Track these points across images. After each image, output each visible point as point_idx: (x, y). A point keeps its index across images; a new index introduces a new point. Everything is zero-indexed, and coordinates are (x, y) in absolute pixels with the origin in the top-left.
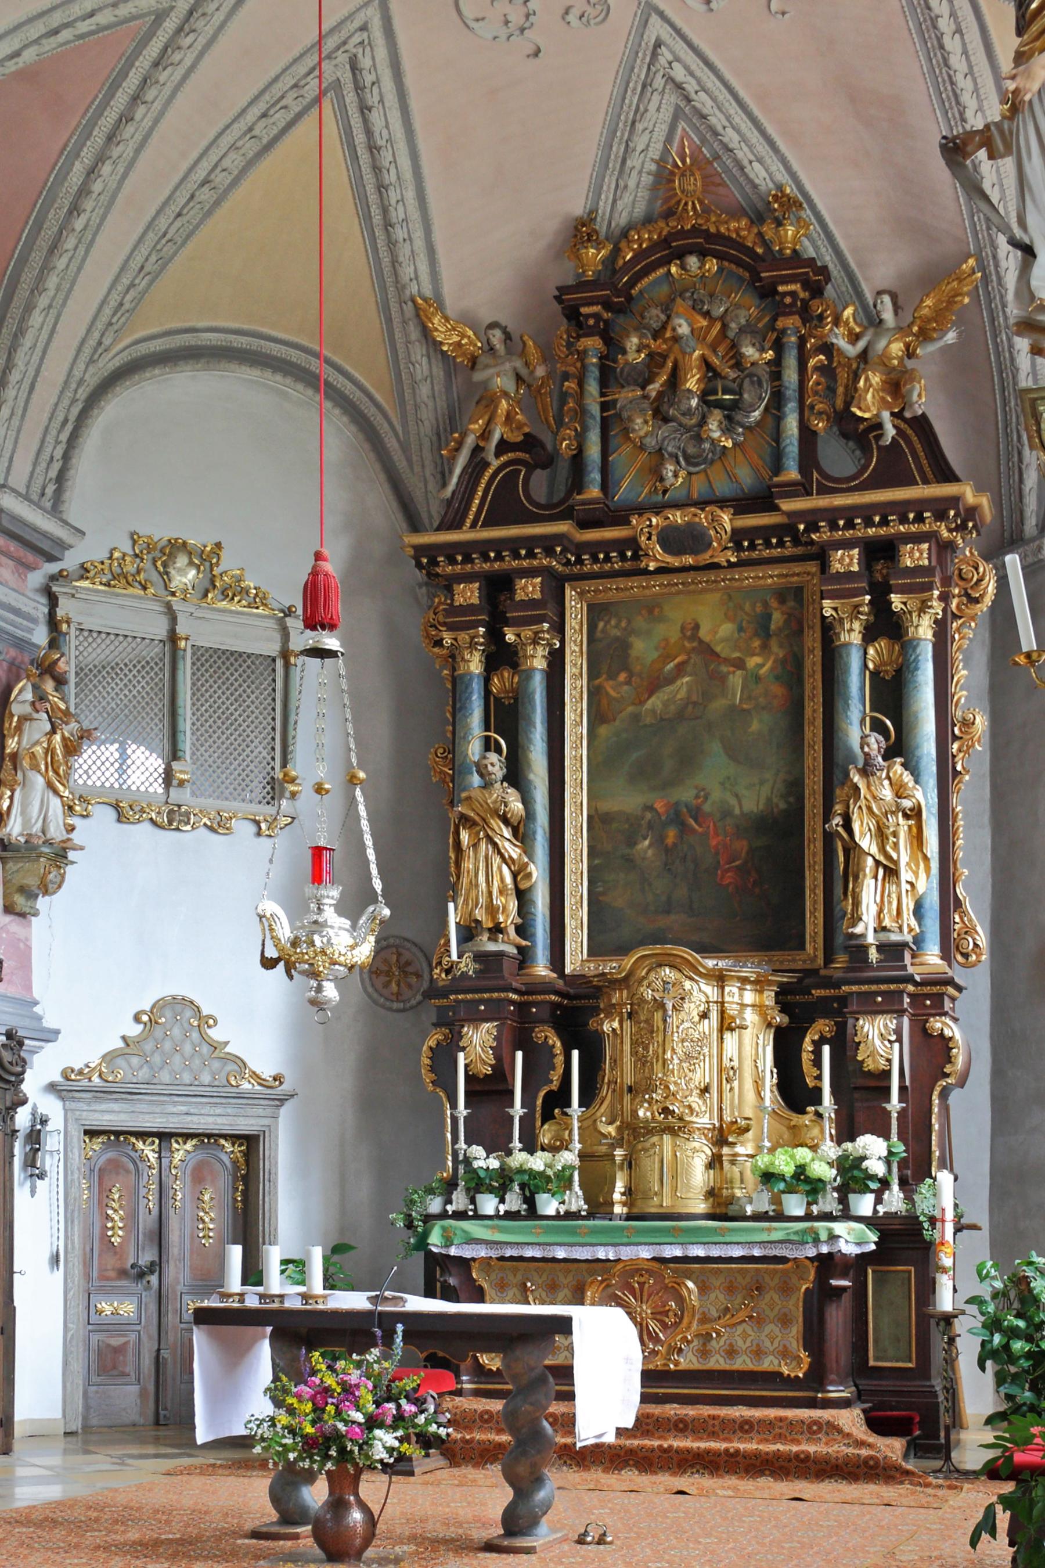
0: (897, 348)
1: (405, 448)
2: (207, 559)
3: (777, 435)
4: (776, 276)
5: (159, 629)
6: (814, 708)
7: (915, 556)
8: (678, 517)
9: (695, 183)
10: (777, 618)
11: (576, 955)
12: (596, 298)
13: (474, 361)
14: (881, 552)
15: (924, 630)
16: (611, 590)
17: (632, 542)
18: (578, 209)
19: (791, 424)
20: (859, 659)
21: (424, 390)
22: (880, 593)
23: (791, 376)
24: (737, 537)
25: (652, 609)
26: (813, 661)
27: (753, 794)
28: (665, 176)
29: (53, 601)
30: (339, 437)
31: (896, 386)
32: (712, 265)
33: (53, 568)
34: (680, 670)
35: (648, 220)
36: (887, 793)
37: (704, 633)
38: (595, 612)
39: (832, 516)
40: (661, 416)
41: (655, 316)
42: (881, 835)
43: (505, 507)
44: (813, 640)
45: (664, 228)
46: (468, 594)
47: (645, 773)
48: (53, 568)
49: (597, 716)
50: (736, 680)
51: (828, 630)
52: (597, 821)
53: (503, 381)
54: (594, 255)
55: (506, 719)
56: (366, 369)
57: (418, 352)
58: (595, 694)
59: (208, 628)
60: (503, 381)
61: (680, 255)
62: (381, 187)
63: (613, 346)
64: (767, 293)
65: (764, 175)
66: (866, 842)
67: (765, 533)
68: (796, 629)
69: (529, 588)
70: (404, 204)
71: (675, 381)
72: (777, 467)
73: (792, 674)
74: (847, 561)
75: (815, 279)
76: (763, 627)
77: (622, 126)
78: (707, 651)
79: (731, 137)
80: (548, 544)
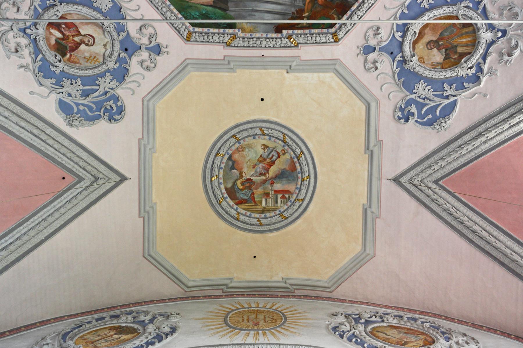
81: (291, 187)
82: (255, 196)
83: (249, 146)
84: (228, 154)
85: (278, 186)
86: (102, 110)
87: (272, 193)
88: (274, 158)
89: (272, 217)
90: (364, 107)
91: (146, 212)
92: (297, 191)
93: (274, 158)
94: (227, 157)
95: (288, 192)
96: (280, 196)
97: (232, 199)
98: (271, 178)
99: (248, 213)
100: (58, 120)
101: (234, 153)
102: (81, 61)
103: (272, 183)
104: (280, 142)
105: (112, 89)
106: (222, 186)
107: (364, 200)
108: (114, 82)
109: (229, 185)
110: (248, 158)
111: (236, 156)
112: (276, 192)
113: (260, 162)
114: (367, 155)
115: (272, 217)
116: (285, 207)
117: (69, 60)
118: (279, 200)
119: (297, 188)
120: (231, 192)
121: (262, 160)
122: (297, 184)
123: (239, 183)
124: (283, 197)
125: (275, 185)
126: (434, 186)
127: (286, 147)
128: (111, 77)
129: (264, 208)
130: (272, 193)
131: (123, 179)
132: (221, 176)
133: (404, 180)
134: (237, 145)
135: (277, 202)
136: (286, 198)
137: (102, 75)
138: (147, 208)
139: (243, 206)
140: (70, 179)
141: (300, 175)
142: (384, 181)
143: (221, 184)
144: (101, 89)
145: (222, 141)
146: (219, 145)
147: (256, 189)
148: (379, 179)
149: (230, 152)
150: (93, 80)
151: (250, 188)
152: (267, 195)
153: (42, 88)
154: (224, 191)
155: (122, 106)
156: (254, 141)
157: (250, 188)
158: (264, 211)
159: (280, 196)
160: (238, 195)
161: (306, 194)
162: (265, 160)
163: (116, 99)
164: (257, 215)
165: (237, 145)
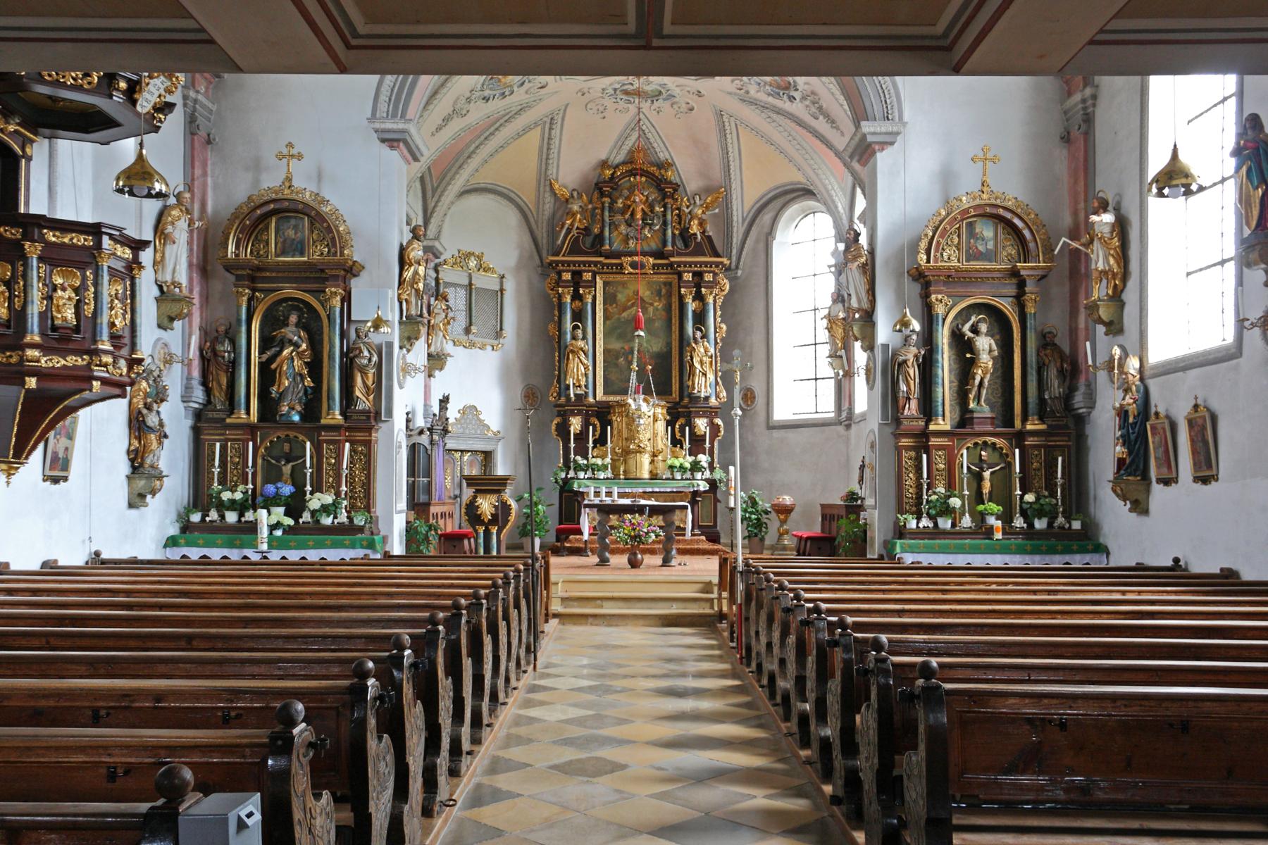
0: (700, 212)
1: (536, 222)
2: (479, 258)
3: (665, 234)
4: (665, 188)
5: (466, 282)
6: (675, 321)
7: (708, 277)
8: (636, 258)
9: (641, 155)
10: (664, 291)
12: (605, 186)
13: (567, 200)
14: (698, 275)
15: (710, 300)
16: (611, 278)
17: (621, 265)
18: (604, 157)
19: (669, 232)
20: (691, 306)
21: (547, 206)
22: (698, 286)
23: (669, 217)
24: (654, 265)
25: (624, 284)
26: (675, 306)
27: (657, 346)
28: (631, 152)
29: (437, 272)
31: (701, 223)
32: (644, 179)
33: (437, 261)
34: (633, 305)
35: (624, 163)
36: (702, 350)
37: (641, 293)
38: (606, 284)
39: (685, 264)
41: (626, 193)
42: (701, 363)
43: (575, 249)
44: (675, 300)
45: (629, 167)
46: (567, 276)
47: (621, 337)
48: (437, 261)
49: (606, 318)
50: (651, 309)
51: (681, 298)
52: (606, 351)
53: (576, 208)
54: (608, 173)
55: (578, 316)
56: (528, 197)
57: (548, 195)
58: (605, 310)
60: (576, 208)
61: (635, 175)
62: (548, 149)
63: (613, 202)
64: (660, 189)
65: (663, 156)
66: (697, 365)
67: (662, 265)
68: (669, 295)
70: (554, 155)
71: (633, 214)
72: (665, 244)
73: (668, 308)
74: (688, 277)
75: (676, 187)
76: (659, 293)
77: (623, 137)
78: (642, 299)
79: (655, 145)
80: (596, 263)
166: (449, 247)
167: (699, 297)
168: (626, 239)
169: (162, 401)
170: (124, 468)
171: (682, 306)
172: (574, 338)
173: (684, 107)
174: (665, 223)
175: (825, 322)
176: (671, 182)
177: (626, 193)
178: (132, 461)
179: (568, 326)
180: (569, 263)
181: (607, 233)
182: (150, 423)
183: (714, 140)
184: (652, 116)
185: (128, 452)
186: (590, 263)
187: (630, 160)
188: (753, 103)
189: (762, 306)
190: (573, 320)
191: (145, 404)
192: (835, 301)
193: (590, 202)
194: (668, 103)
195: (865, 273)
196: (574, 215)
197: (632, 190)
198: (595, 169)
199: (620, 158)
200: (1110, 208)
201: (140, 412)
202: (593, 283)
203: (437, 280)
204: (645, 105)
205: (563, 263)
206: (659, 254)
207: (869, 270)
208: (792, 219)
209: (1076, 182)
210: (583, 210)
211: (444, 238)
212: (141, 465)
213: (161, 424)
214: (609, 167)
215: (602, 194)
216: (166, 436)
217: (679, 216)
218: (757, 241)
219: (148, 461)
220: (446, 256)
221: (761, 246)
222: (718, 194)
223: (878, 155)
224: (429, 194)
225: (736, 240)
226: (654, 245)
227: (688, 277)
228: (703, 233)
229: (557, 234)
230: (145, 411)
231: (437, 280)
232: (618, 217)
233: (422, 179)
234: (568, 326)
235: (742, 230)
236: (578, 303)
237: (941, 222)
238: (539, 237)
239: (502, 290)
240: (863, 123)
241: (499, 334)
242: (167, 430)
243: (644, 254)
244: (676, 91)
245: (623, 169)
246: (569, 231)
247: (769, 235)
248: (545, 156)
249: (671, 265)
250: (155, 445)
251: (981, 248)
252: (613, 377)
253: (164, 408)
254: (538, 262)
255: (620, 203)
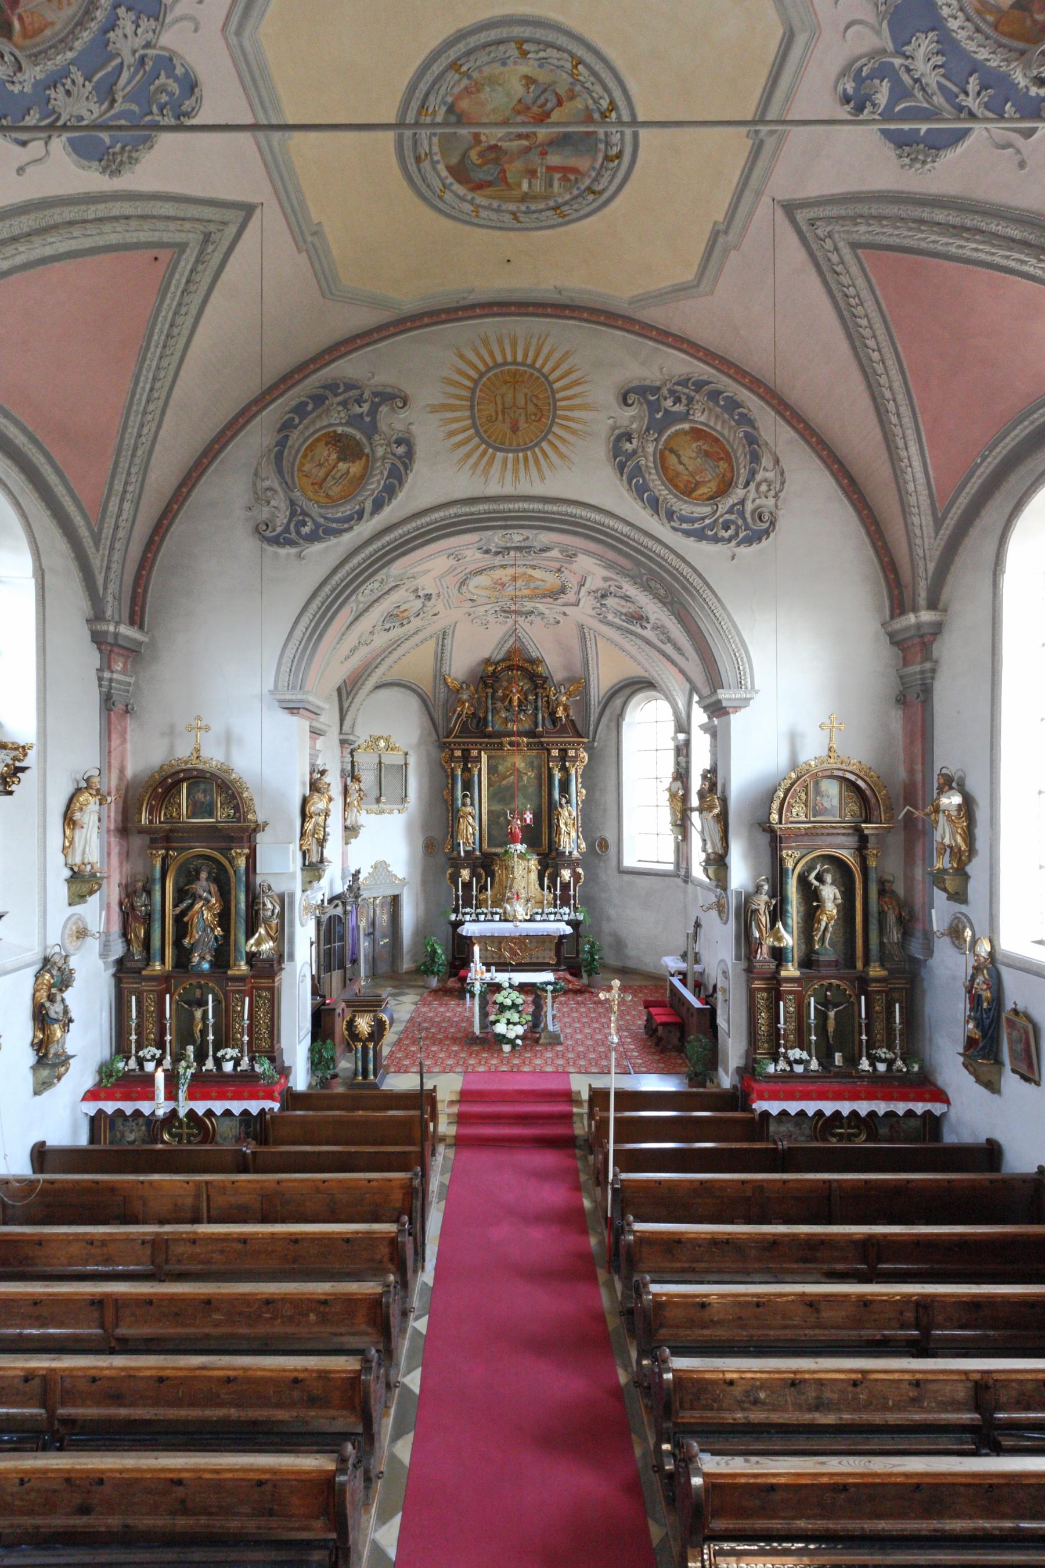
6: (545, 788)
7: (571, 753)
11: (485, 846)
12: (489, 678)
14: (563, 752)
15: (573, 771)
16: (494, 753)
17: (501, 744)
18: (487, 656)
20: (557, 775)
24: (528, 744)
25: (504, 758)
26: (545, 776)
28: (509, 652)
30: (413, 703)
31: (566, 709)
35: (503, 660)
39: (553, 743)
40: (508, 710)
41: (505, 684)
42: (566, 824)
44: (545, 771)
45: (508, 663)
46: (458, 753)
47: (503, 800)
49: (490, 785)
50: (525, 778)
51: (550, 770)
52: (490, 812)
53: (465, 697)
54: (491, 669)
55: (467, 786)
56: (427, 687)
59: (389, 759)
60: (465, 697)
63: (495, 691)
65: (534, 655)
67: (535, 744)
69: (474, 753)
71: (511, 701)
72: (536, 725)
73: (539, 777)
74: (555, 753)
75: (545, 680)
81: (582, 163)
82: (508, 175)
83: (493, 81)
84: (445, 103)
85: (554, 159)
86: (155, 109)
87: (541, 171)
88: (549, 106)
89: (541, 211)
90: (781, 32)
91: (307, 237)
92: (593, 174)
93: (549, 106)
94: (444, 109)
95: (574, 170)
96: (557, 176)
97: (460, 182)
98: (540, 145)
99: (495, 204)
100: (93, 180)
101: (458, 98)
102: (50, 16)
103: (544, 154)
104: (565, 76)
105: (148, 45)
106: (441, 167)
107: (720, 216)
108: (144, 23)
109: (454, 161)
110: (489, 107)
111: (464, 104)
112: (551, 169)
113: (519, 113)
114: (751, 142)
115: (541, 211)
116: (567, 197)
117: (25, 35)
118: (556, 184)
119: (594, 168)
120: (460, 172)
121: (522, 108)
122: (594, 159)
123: (473, 155)
124: (564, 179)
125: (548, 157)
126: (846, 251)
127: (578, 88)
128: (132, 16)
129: (526, 194)
130: (541, 171)
131: (248, 210)
132: (436, 149)
133: (801, 216)
134: (465, 82)
135: (551, 186)
136: (569, 180)
137: (111, 25)
138: (309, 239)
139: (487, 191)
140: (165, 255)
141: (602, 146)
142: (766, 199)
143: (438, 162)
144: (129, 59)
145: (429, 78)
146: (423, 87)
147: (511, 162)
148: (759, 194)
149: (449, 99)
150: (101, 50)
151: (496, 161)
152: (532, 173)
153: (31, 145)
154: (444, 173)
155: (187, 73)
156: (502, 69)
157: (496, 161)
158: (524, 198)
159: (557, 176)
160: (472, 175)
161: (610, 182)
162: (528, 108)
163: (167, 62)
164: (512, 207)
165: (465, 82)
166: (361, 736)
167: (564, 769)
168: (506, 721)
169: (67, 987)
170: (30, 1057)
171: (551, 777)
172: (464, 804)
173: (552, 620)
174: (536, 708)
175: (667, 795)
176: (541, 676)
177: (505, 684)
178: (38, 1051)
179: (459, 794)
180: (459, 744)
181: (490, 718)
182: (53, 1015)
183: (576, 644)
184: (526, 626)
185: (32, 1045)
186: (476, 743)
187: (507, 658)
188: (610, 624)
189: (614, 771)
190: (464, 789)
191: (49, 997)
192: (675, 779)
193: (477, 691)
194: (539, 618)
195: (719, 822)
196: (463, 703)
197: (510, 681)
198: (479, 664)
199: (500, 656)
200: (954, 785)
201: (42, 1005)
202: (478, 759)
203: (353, 762)
204: (521, 620)
205: (455, 743)
206: (531, 734)
207: (723, 818)
208: (639, 704)
209: (912, 742)
210: (471, 698)
211: (358, 731)
212: (46, 1055)
213: (66, 1011)
214: (491, 664)
215: (486, 685)
216: (71, 1021)
217: (548, 702)
218: (610, 720)
219: (52, 1051)
220: (361, 741)
221: (613, 724)
222: (579, 684)
223: (732, 716)
224: (344, 696)
225: (593, 718)
226: (527, 726)
227: (555, 753)
228: (568, 716)
229: (449, 720)
230: (48, 1004)
231: (353, 762)
232: (499, 704)
233: (339, 690)
234: (459, 794)
235: (598, 711)
236: (466, 774)
237: (792, 785)
238: (436, 716)
239: (406, 764)
240: (719, 691)
241: (404, 799)
242: (73, 1014)
243: (520, 734)
244: (547, 612)
245: (503, 665)
246: (460, 715)
247: (620, 717)
248: (440, 657)
249: (542, 743)
250: (59, 1033)
251: (826, 805)
252: (495, 833)
253: (69, 995)
254: (435, 737)
255: (500, 693)
